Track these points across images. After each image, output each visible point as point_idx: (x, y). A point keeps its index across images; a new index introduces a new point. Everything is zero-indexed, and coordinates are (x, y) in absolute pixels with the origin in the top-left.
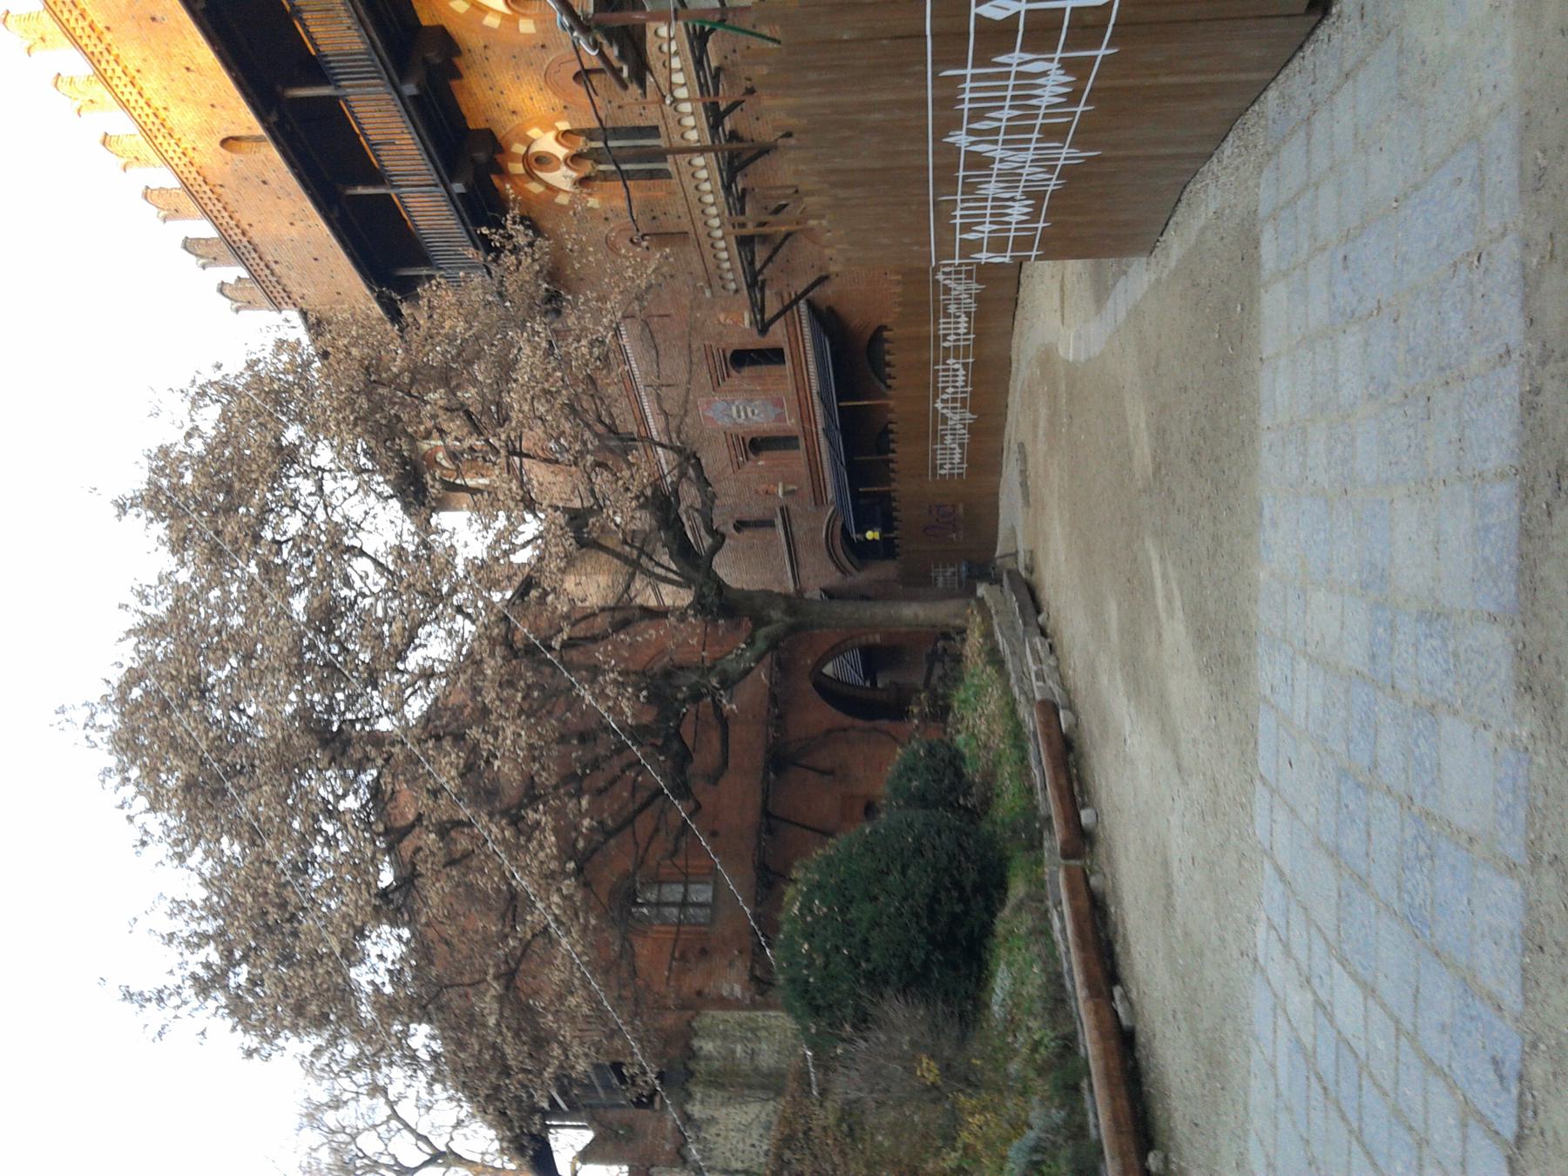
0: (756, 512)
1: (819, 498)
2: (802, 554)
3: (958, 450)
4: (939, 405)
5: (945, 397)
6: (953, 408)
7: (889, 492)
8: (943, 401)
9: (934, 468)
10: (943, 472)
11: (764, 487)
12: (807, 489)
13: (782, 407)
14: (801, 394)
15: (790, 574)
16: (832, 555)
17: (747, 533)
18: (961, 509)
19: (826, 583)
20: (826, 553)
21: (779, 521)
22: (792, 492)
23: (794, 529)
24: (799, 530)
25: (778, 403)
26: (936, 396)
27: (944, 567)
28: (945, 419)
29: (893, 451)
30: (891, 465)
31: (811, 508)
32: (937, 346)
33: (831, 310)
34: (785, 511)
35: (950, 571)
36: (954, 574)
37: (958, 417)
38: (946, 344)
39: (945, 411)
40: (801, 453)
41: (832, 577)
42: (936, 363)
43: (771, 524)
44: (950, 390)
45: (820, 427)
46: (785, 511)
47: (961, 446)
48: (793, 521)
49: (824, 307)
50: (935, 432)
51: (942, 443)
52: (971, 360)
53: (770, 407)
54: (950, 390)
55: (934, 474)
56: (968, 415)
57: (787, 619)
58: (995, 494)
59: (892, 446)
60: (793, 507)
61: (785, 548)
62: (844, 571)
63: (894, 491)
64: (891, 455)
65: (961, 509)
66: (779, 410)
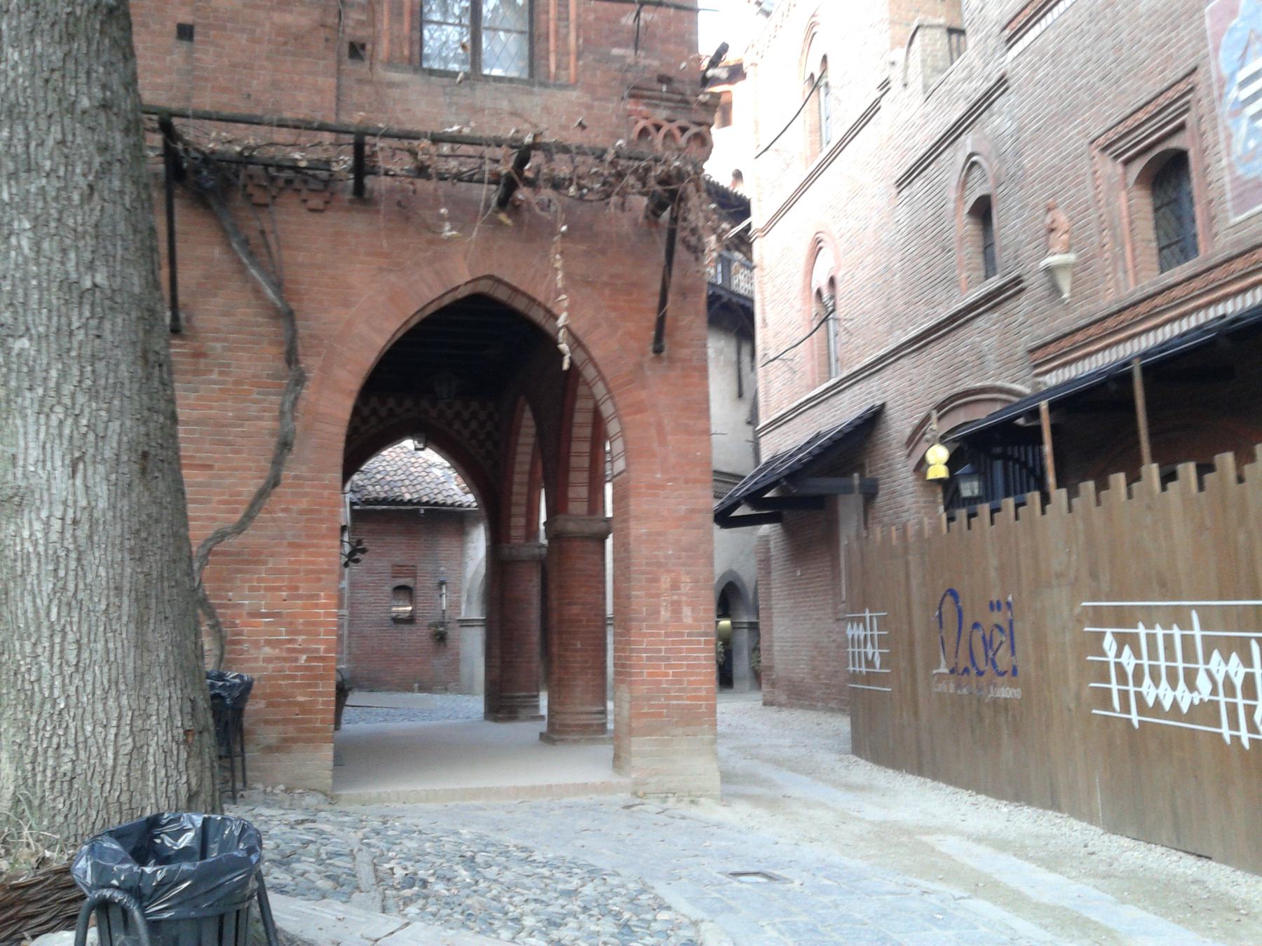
2: (937, 351)
3: (1186, 699)
7: (1041, 485)
9: (1121, 618)
10: (1109, 643)
11: (1062, 218)
12: (1064, 323)
17: (963, 226)
20: (941, 397)
21: (994, 282)
22: (1055, 290)
23: (980, 322)
27: (883, 641)
29: (1168, 477)
30: (1119, 479)
34: (1015, 287)
46: (1015, 287)
47: (1207, 711)
48: (995, 315)
51: (1210, 645)
55: (1099, 617)
59: (1188, 470)
60: (1023, 304)
63: (1045, 499)
64: (1152, 471)
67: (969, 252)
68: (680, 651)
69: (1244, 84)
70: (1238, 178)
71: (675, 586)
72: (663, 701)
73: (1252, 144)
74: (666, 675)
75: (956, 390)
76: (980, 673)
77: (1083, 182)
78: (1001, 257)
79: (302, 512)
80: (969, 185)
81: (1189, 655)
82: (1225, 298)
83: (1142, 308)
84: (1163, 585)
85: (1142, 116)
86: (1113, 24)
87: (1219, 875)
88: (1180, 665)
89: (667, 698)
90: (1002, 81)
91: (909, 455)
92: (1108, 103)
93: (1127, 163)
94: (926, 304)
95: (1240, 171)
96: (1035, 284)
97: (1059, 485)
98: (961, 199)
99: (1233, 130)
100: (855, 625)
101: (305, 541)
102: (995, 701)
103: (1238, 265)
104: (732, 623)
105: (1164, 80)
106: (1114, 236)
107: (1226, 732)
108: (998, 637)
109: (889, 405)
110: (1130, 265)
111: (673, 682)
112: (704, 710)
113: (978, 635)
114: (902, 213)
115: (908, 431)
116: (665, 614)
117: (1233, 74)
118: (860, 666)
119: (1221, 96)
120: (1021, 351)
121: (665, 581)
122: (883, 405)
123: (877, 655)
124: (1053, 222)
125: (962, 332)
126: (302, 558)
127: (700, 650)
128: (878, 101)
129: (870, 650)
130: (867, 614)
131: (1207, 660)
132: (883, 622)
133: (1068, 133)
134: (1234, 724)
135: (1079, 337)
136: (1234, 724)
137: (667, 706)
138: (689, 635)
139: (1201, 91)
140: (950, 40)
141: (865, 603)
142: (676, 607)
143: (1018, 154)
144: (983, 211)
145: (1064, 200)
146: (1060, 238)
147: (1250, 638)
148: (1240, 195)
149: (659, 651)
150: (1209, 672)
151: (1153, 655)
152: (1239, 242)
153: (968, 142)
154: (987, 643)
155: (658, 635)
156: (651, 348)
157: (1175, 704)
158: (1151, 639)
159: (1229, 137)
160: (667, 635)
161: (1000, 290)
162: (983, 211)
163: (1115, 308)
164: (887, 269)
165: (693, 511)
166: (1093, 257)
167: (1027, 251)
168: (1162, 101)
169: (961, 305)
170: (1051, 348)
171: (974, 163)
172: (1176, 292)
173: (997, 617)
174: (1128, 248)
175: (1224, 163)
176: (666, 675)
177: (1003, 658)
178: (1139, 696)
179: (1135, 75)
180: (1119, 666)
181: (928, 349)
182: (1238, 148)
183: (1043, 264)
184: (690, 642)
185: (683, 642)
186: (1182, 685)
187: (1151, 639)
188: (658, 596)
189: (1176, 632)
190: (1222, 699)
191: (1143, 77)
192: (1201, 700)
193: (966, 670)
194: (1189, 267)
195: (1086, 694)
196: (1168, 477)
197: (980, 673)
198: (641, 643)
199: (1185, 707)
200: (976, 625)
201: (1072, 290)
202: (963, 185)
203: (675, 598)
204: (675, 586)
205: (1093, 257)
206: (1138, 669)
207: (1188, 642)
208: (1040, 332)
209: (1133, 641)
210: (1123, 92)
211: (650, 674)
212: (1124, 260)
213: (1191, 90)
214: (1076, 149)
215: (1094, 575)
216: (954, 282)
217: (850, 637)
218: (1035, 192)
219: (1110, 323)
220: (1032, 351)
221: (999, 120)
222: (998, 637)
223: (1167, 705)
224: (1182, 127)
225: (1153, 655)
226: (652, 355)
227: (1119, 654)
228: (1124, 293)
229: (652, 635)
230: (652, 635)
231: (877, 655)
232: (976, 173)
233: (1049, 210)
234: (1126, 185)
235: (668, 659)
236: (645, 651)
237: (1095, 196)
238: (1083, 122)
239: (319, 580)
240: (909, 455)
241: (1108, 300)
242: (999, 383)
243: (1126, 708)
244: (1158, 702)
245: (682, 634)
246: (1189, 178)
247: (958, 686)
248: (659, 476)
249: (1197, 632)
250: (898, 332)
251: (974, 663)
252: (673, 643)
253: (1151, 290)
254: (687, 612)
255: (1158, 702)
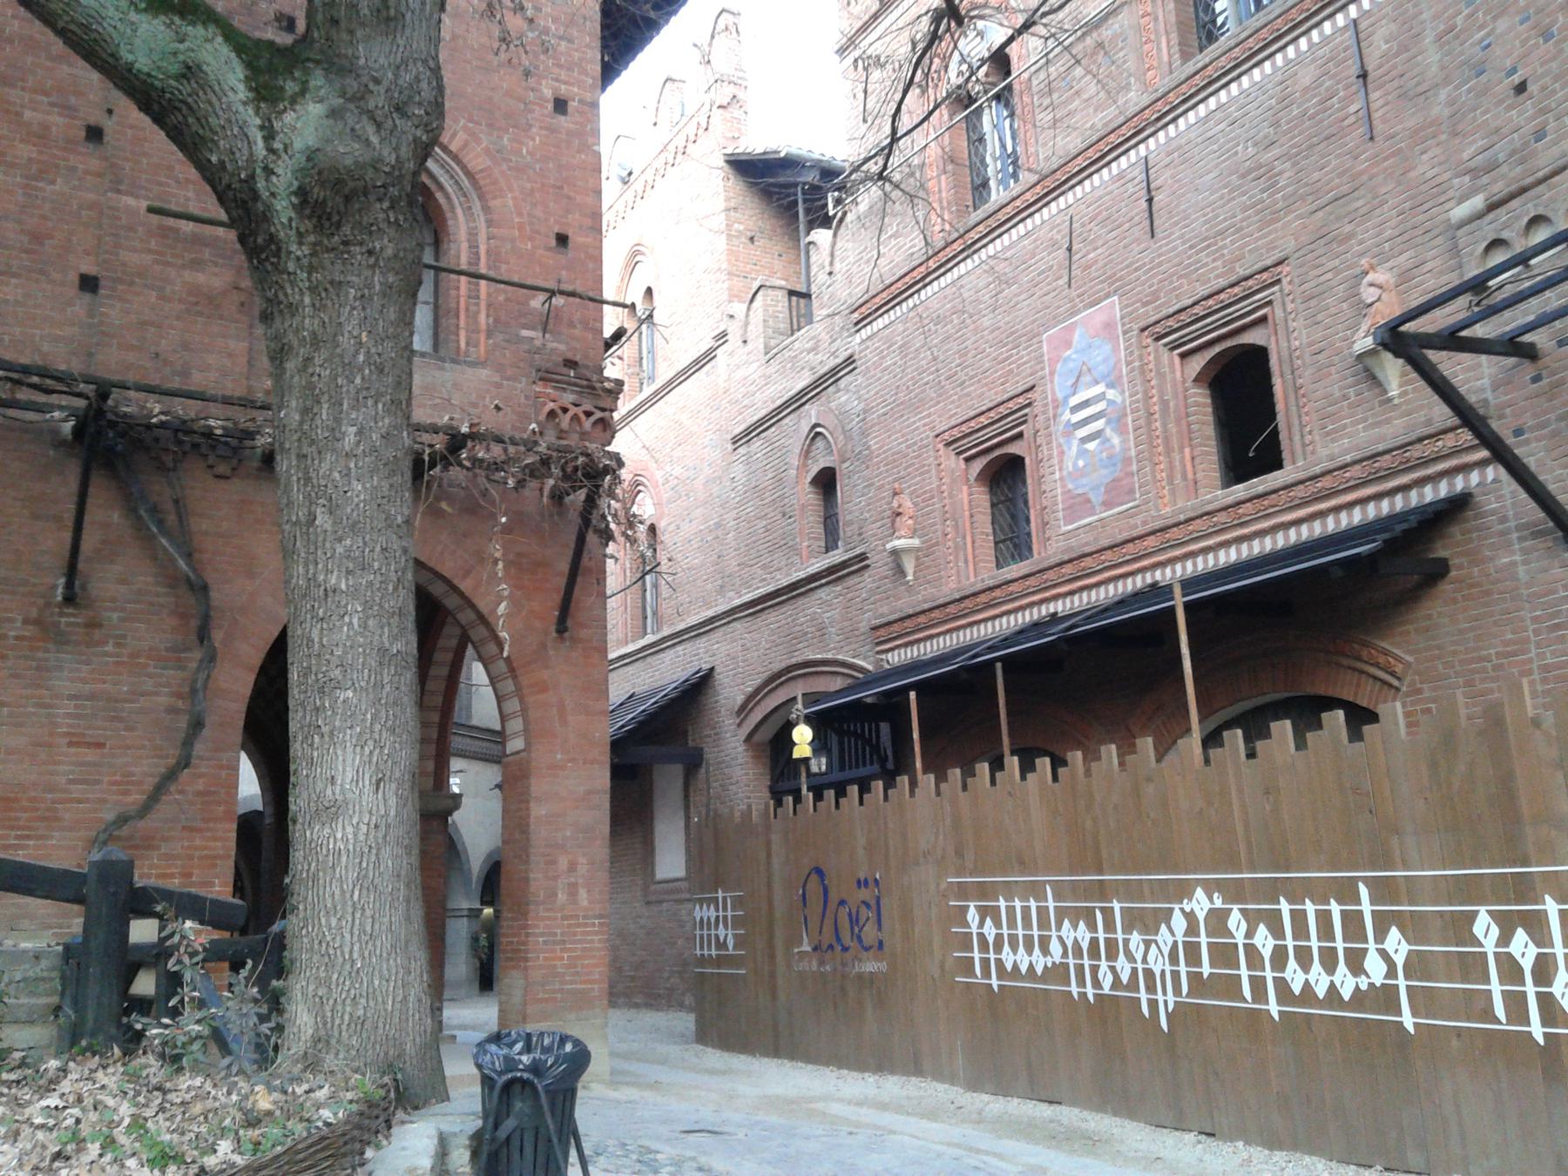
0: (852, 498)
1: (886, 632)
4: (1200, 903)
5: (1236, 923)
6: (1193, 952)
8: (1218, 920)
9: (984, 891)
10: (972, 916)
12: (906, 603)
13: (1108, 505)
14: (1151, 542)
15: (737, 602)
16: (776, 680)
17: (808, 496)
18: (870, 966)
19: (723, 679)
20: (778, 666)
21: (837, 557)
22: (900, 571)
23: (822, 594)
24: (825, 605)
25: (1116, 491)
26: (1235, 892)
27: (737, 922)
28: (1148, 923)
30: (984, 768)
31: (867, 619)
32: (1471, 891)
33: (1438, 572)
34: (860, 562)
35: (726, 934)
36: (721, 945)
37: (1158, 963)
38: (1485, 927)
39: (1179, 923)
40: (988, 574)
41: (730, 691)
42: (1383, 891)
43: (831, 544)
44: (1264, 941)
45: (1060, 607)
46: (860, 562)
47: (1058, 972)
49: (1441, 553)
50: (1102, 891)
51: (1061, 914)
52: (1408, 1021)
53: (1104, 475)
54: (1264, 941)
55: (963, 892)
56: (1167, 1000)
57: (285, 177)
58: (914, 1066)
59: (1044, 763)
60: (867, 580)
61: (785, 582)
62: (744, 710)
63: (913, 784)
64: (1013, 762)
65: (870, 966)
66: (1096, 498)
67: (811, 522)
68: (575, 934)
69: (1075, 409)
70: (1069, 491)
71: (572, 867)
72: (557, 986)
73: (1081, 463)
74: (562, 959)
75: (794, 661)
76: (845, 949)
77: (928, 471)
78: (845, 531)
79: (199, 794)
80: (812, 454)
81: (1044, 923)
82: (1055, 598)
83: (983, 598)
84: (1022, 862)
85: (984, 420)
86: (960, 329)
87: (1069, 1115)
88: (1036, 933)
89: (563, 982)
90: (850, 360)
91: (739, 725)
92: (953, 402)
93: (967, 460)
94: (764, 567)
95: (1070, 486)
96: (879, 563)
97: (926, 770)
98: (803, 467)
99: (1065, 448)
100: (705, 907)
101: (199, 824)
102: (860, 976)
103: (1068, 570)
104: (495, 911)
105: (1005, 391)
106: (956, 527)
107: (1074, 989)
108: (864, 912)
109: (718, 670)
110: (970, 558)
111: (569, 966)
112: (596, 993)
113: (844, 911)
114: (738, 470)
115: (740, 699)
116: (562, 897)
117: (1066, 398)
118: (709, 948)
119: (1055, 416)
120: (864, 627)
121: (563, 863)
122: (712, 669)
123: (730, 936)
124: (900, 506)
125: (800, 601)
126: (198, 842)
127: (596, 933)
128: (712, 350)
129: (721, 932)
130: (720, 894)
131: (1059, 928)
132: (738, 903)
133: (915, 422)
134: (1081, 982)
135: (922, 619)
136: (1081, 982)
137: (561, 991)
138: (585, 917)
139: (1038, 408)
140: (790, 301)
141: (718, 882)
142: (572, 891)
143: (864, 434)
144: (826, 482)
145: (909, 487)
146: (906, 522)
147: (1094, 908)
148: (1070, 507)
149: (556, 934)
150: (1060, 938)
151: (1012, 923)
152: (1070, 549)
153: (812, 412)
154: (854, 920)
155: (555, 918)
156: (553, 628)
157: (1031, 967)
158: (1011, 911)
159: (1062, 453)
160: (563, 918)
161: (844, 565)
162: (826, 482)
163: (957, 596)
164: (718, 525)
165: (589, 792)
166: (937, 544)
167: (872, 529)
168: (1003, 410)
169: (802, 575)
170: (896, 627)
171: (819, 434)
172: (1013, 587)
173: (864, 894)
174: (969, 539)
175: (1057, 476)
176: (562, 959)
177: (870, 933)
178: (999, 962)
179: (979, 381)
180: (981, 936)
181: (764, 616)
182: (1069, 465)
183: (889, 546)
184: (586, 925)
185: (579, 925)
186: (1037, 950)
187: (1011, 911)
188: (555, 878)
189: (1033, 904)
190: (1071, 961)
191: (986, 384)
192: (1054, 963)
193: (831, 947)
194: (1025, 567)
195: (949, 964)
196: (1027, 767)
197: (845, 949)
198: (537, 926)
199: (1039, 970)
200: (842, 902)
201: (915, 573)
202: (806, 453)
203: (573, 880)
204: (572, 867)
205: (937, 544)
206: (999, 937)
207: (1042, 912)
208: (885, 610)
209: (994, 913)
210: (968, 395)
211: (546, 959)
212: (966, 549)
213: (1029, 405)
214: (922, 440)
215: (959, 853)
216: (794, 549)
217: (698, 919)
218: (881, 473)
219: (951, 609)
220: (875, 629)
221: (846, 397)
222: (864, 912)
223: (1024, 968)
224: (1020, 436)
225: (1012, 923)
226: (554, 635)
227: (981, 925)
228: (965, 583)
229: (548, 918)
230: (548, 918)
231: (730, 936)
232: (820, 443)
233: (895, 494)
234: (968, 480)
235: (564, 942)
236: (542, 935)
237: (939, 486)
238: (929, 415)
239: (214, 866)
240: (739, 725)
241: (949, 588)
242: (840, 657)
243: (986, 972)
244: (1015, 966)
245: (577, 917)
246: (1024, 482)
247: (822, 963)
248: (559, 756)
249: (1051, 904)
250: (732, 594)
251: (838, 939)
252: (569, 926)
253: (991, 583)
254: (583, 894)
255: (1015, 966)
